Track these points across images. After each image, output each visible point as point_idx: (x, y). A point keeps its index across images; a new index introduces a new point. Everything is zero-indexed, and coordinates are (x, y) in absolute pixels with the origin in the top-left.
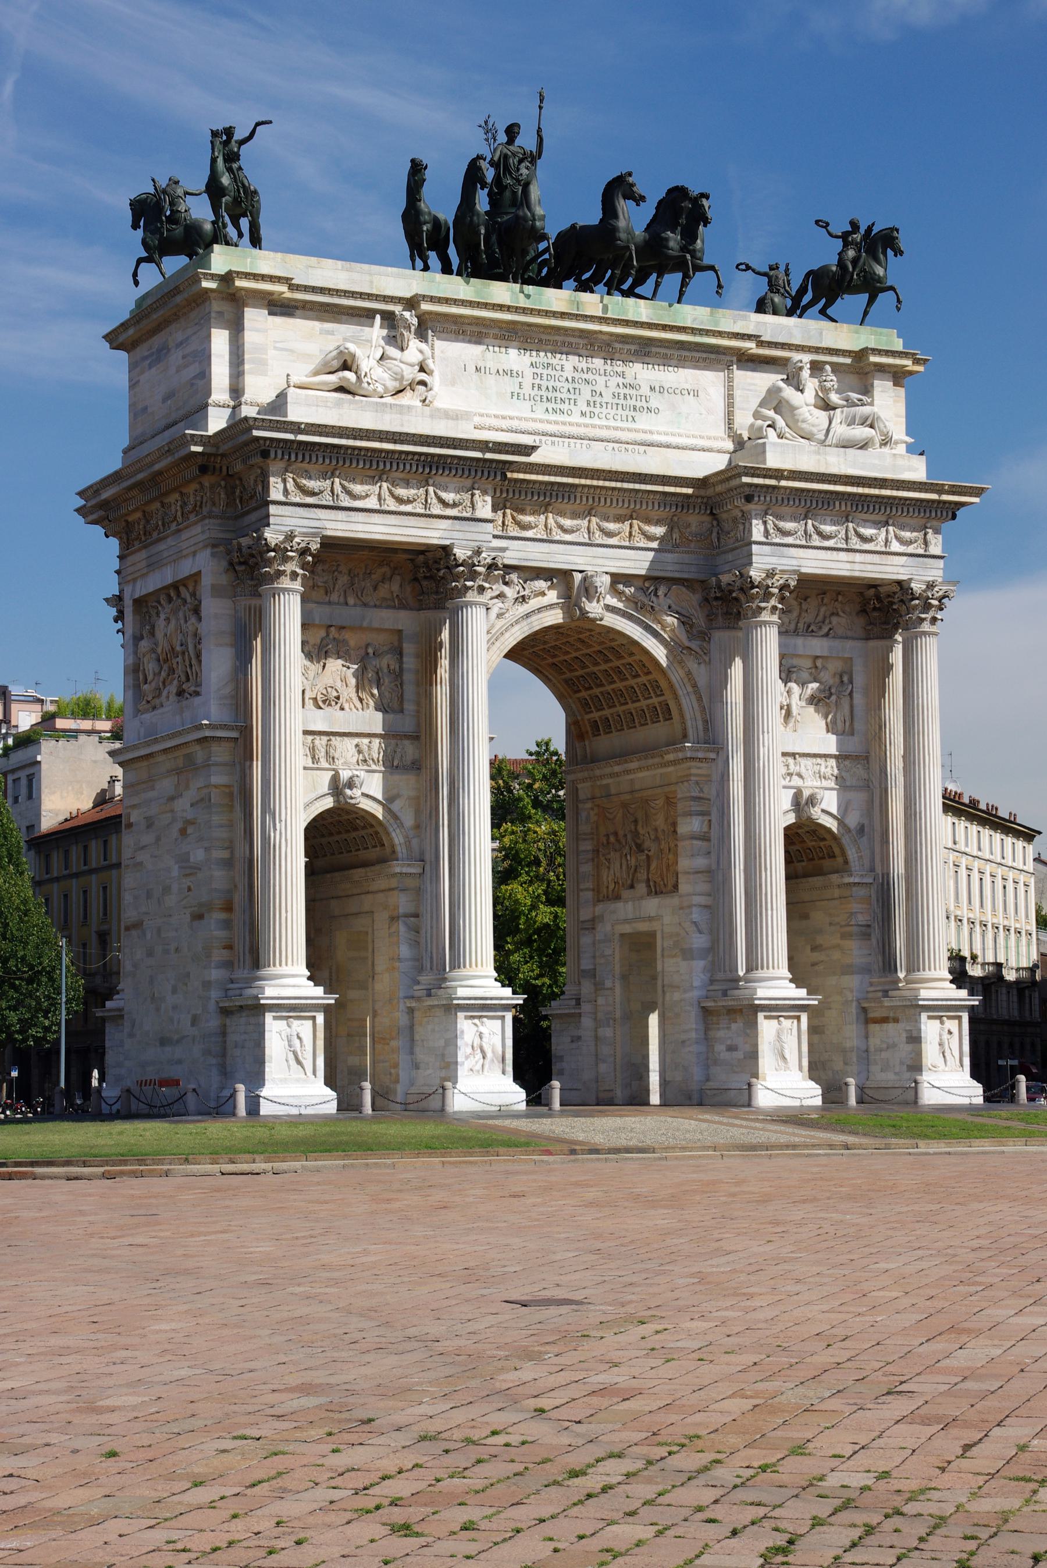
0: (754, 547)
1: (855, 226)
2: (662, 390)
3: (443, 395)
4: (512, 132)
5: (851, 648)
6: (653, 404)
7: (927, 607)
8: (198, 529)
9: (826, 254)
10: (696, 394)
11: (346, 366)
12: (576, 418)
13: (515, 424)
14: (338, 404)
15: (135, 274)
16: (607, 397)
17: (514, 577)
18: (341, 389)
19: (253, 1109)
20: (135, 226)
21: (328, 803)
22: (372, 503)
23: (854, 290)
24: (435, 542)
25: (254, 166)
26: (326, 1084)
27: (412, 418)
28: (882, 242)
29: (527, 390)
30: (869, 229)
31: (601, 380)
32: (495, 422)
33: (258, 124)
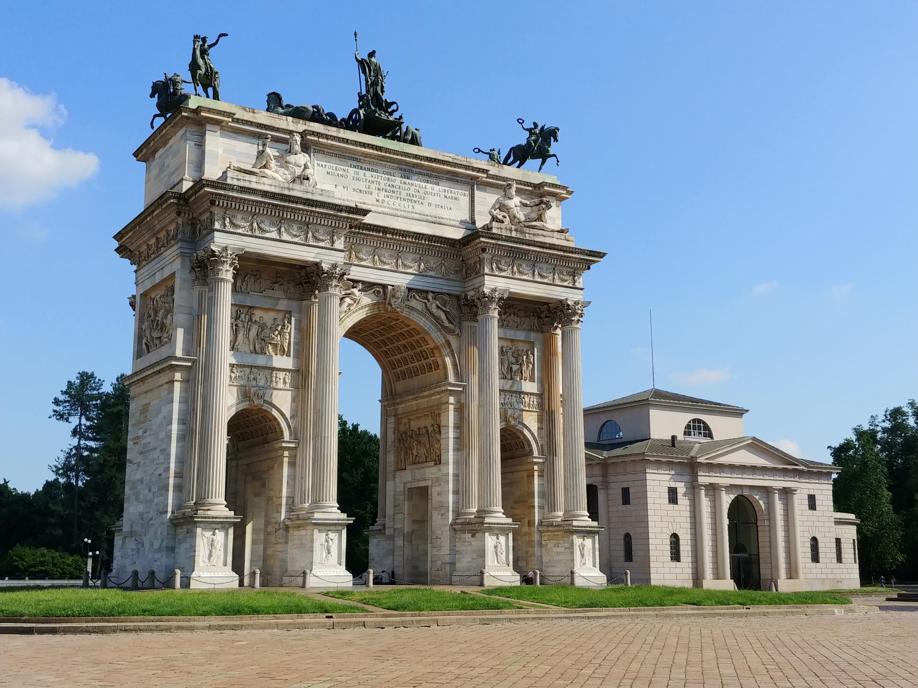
0: (486, 277)
1: (535, 124)
5: (533, 336)
7: (575, 313)
8: (175, 247)
9: (522, 138)
15: (152, 123)
19: (186, 584)
20: (152, 96)
23: (534, 157)
24: (311, 259)
25: (215, 59)
26: (233, 570)
28: (550, 134)
30: (543, 127)
33: (221, 35)
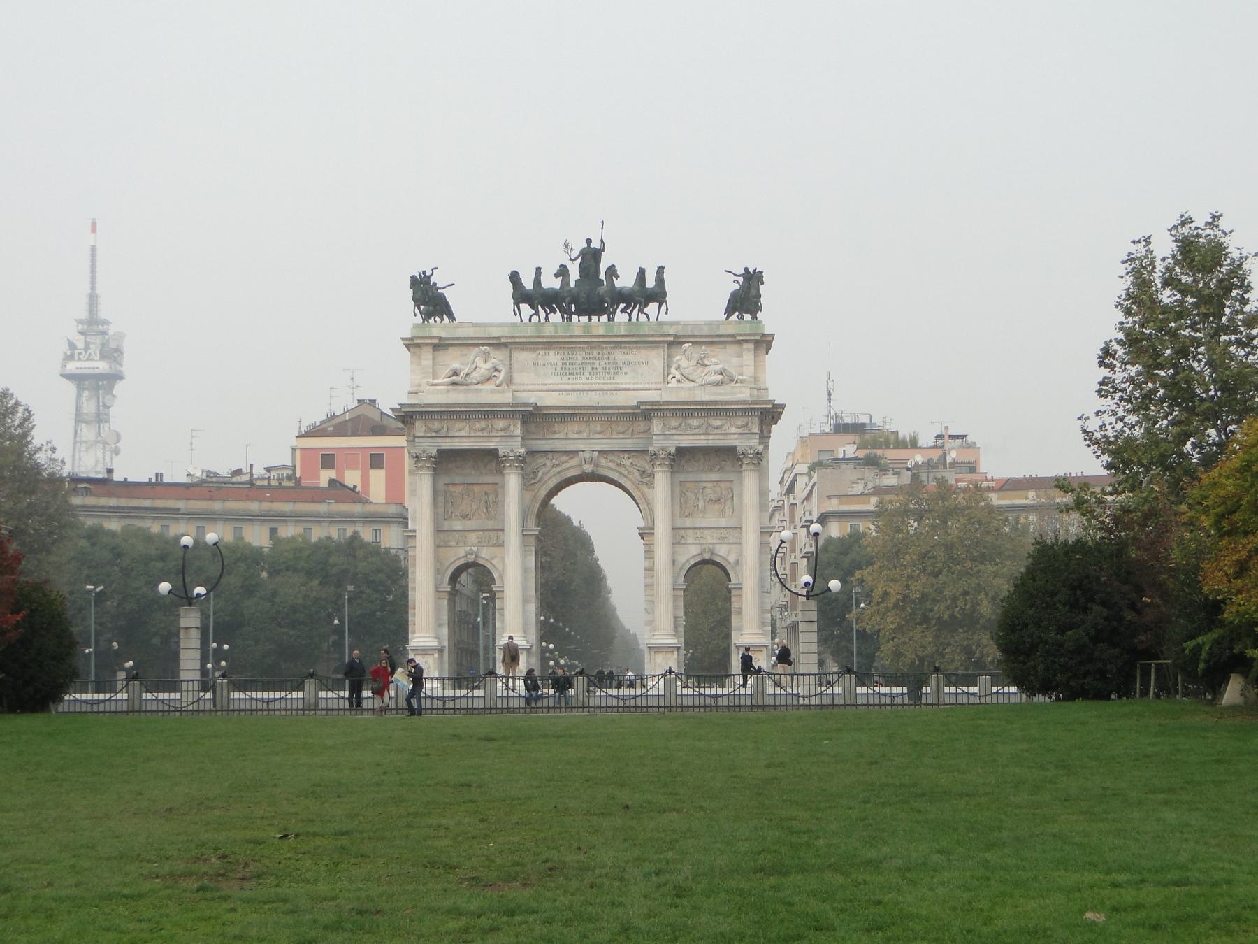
1: (746, 269)
2: (629, 363)
3: (518, 378)
4: (589, 241)
5: (731, 477)
6: (624, 370)
10: (647, 363)
11: (456, 373)
12: (584, 381)
13: (551, 387)
14: (448, 391)
16: (600, 369)
17: (550, 456)
18: (454, 384)
21: (463, 561)
22: (463, 433)
27: (489, 395)
29: (559, 370)
31: (597, 363)
32: (540, 387)
